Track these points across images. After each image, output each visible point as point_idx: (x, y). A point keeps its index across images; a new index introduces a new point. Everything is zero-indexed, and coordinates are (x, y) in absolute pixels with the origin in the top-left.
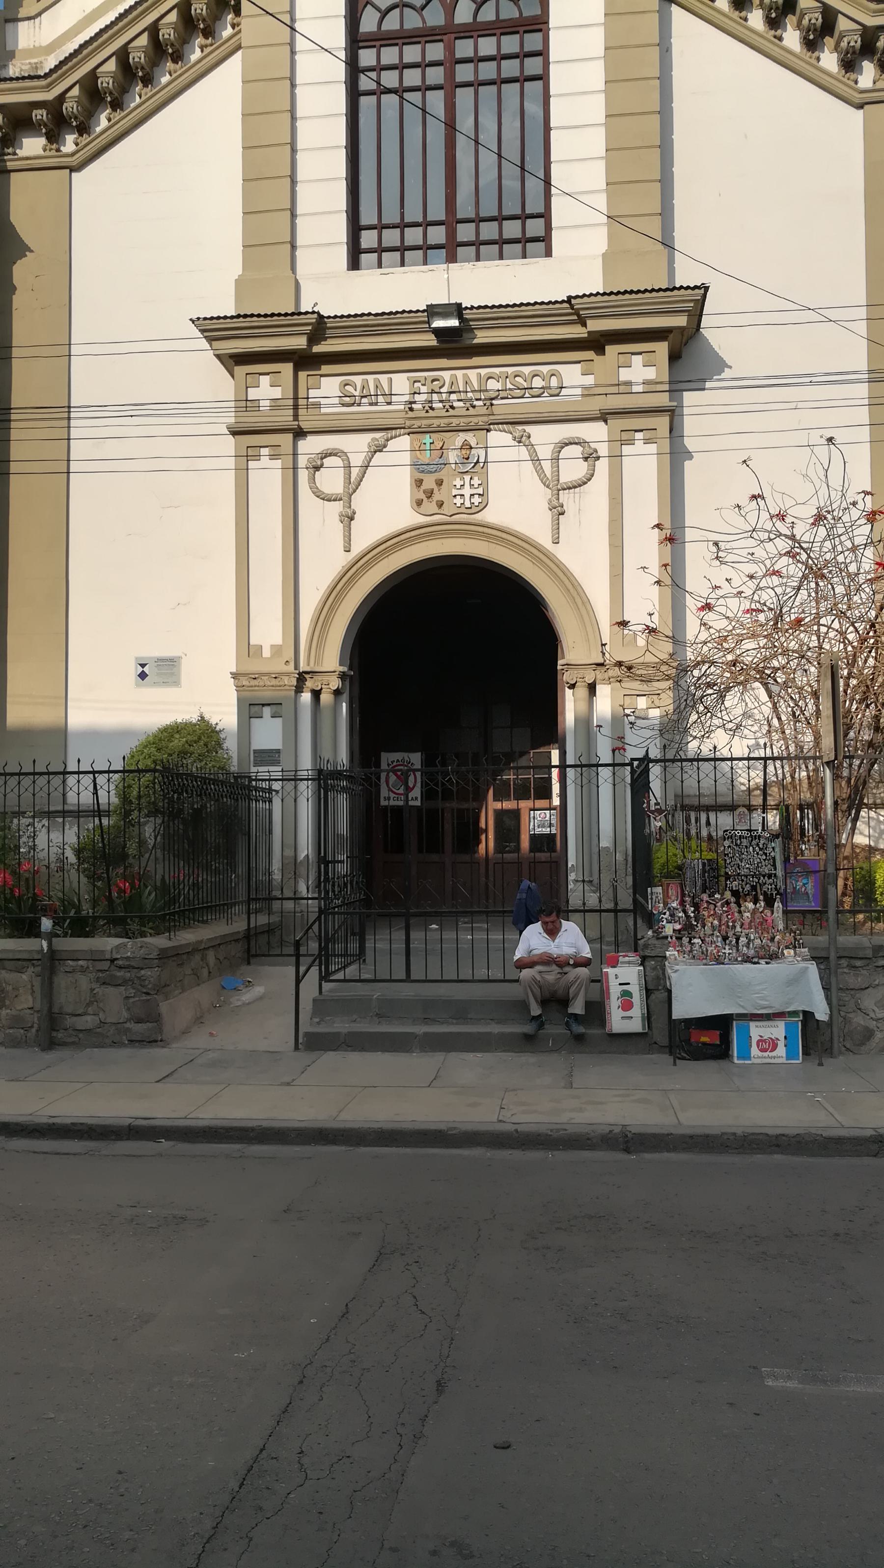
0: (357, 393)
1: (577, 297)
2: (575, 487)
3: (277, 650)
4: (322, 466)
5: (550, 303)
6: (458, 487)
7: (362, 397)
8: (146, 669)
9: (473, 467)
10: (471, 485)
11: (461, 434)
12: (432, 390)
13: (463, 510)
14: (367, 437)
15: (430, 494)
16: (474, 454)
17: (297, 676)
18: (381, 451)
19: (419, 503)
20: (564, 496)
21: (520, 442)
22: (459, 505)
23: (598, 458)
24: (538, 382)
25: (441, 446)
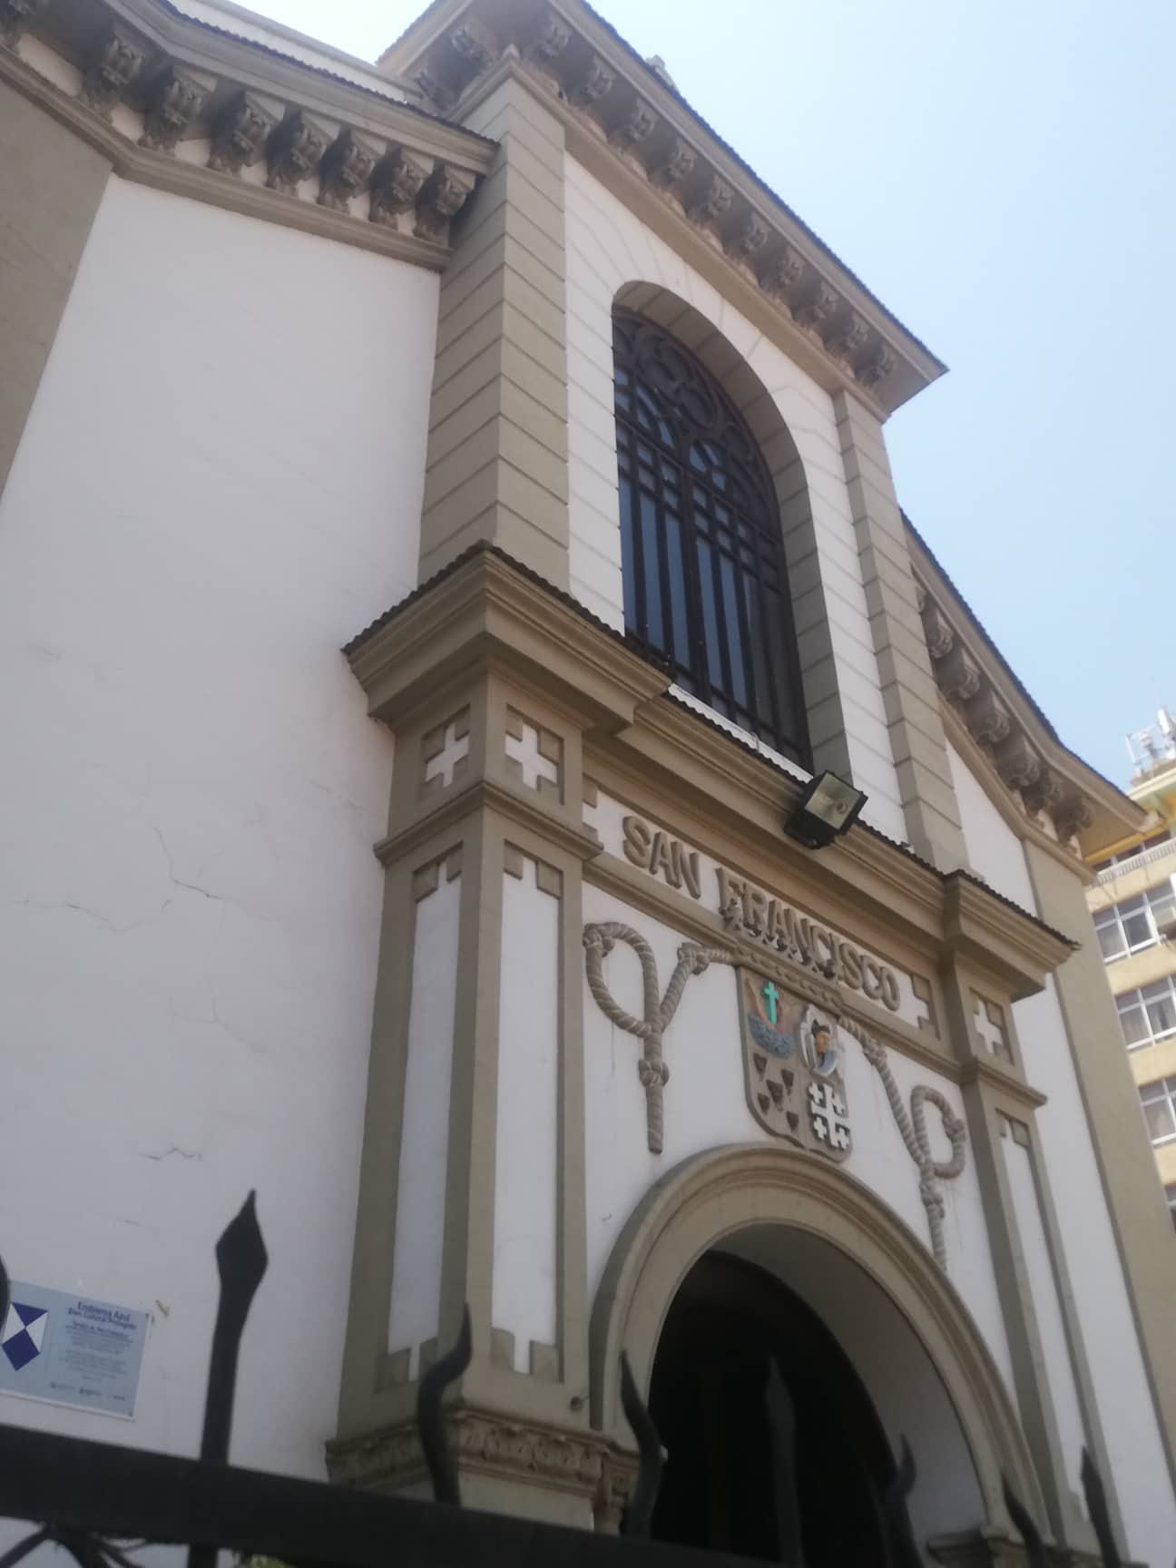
1: (969, 878)
3: (550, 1361)
8: (36, 1330)
9: (830, 1076)
10: (835, 1108)
15: (775, 1092)
18: (697, 972)
19: (764, 1103)
20: (940, 1187)
23: (963, 1138)
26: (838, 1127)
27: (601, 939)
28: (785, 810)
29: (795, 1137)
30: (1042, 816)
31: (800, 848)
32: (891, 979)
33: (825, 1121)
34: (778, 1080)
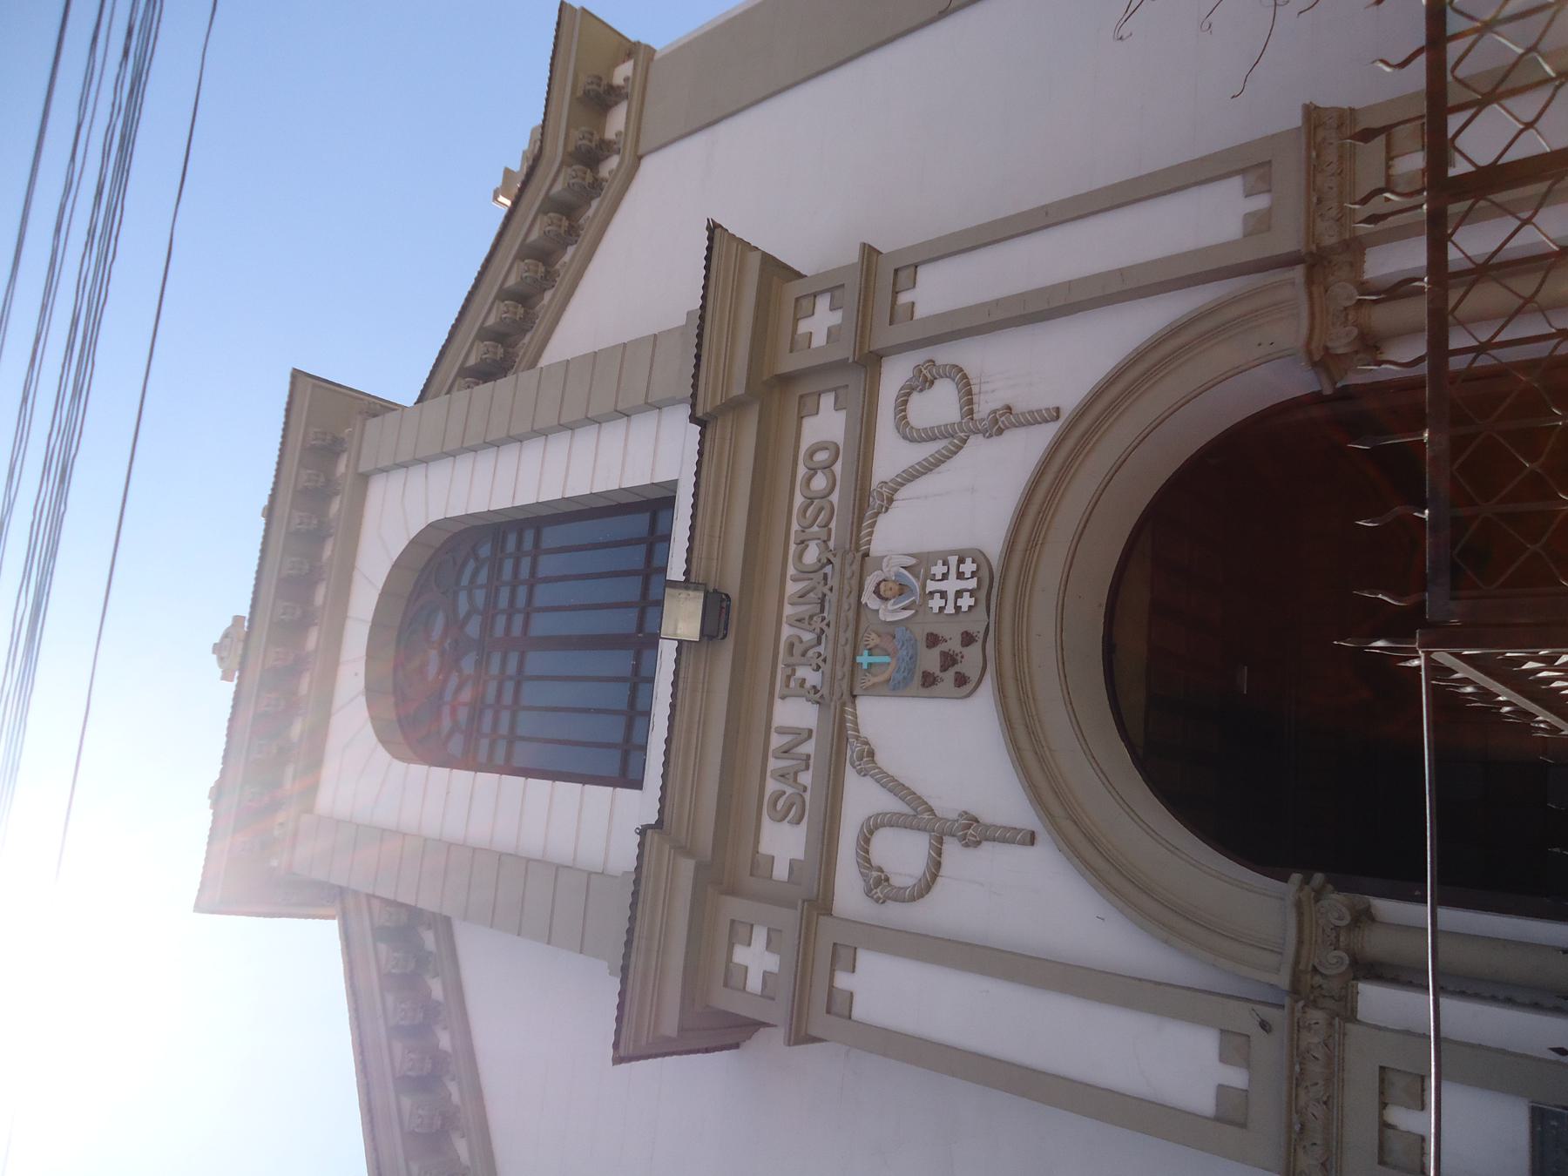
0: (789, 791)
2: (970, 393)
3: (1234, 1048)
4: (880, 870)
5: (700, 453)
6: (942, 602)
7: (795, 780)
9: (916, 576)
10: (945, 577)
11: (864, 600)
12: (804, 655)
13: (983, 594)
14: (851, 779)
16: (898, 575)
17: (1301, 1004)
18: (871, 754)
19: (961, 680)
20: (984, 408)
21: (891, 500)
22: (972, 602)
23: (934, 362)
24: (820, 482)
25: (873, 636)
26: (960, 576)
27: (873, 892)
28: (708, 647)
29: (981, 635)
30: (610, 134)
31: (734, 615)
32: (811, 453)
33: (959, 594)
34: (935, 653)
